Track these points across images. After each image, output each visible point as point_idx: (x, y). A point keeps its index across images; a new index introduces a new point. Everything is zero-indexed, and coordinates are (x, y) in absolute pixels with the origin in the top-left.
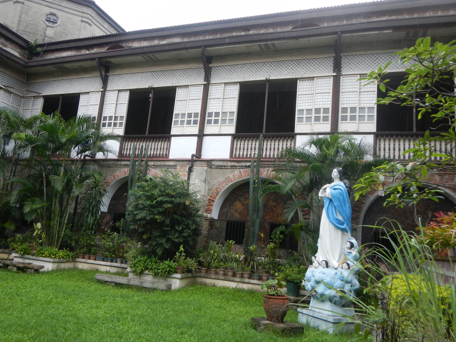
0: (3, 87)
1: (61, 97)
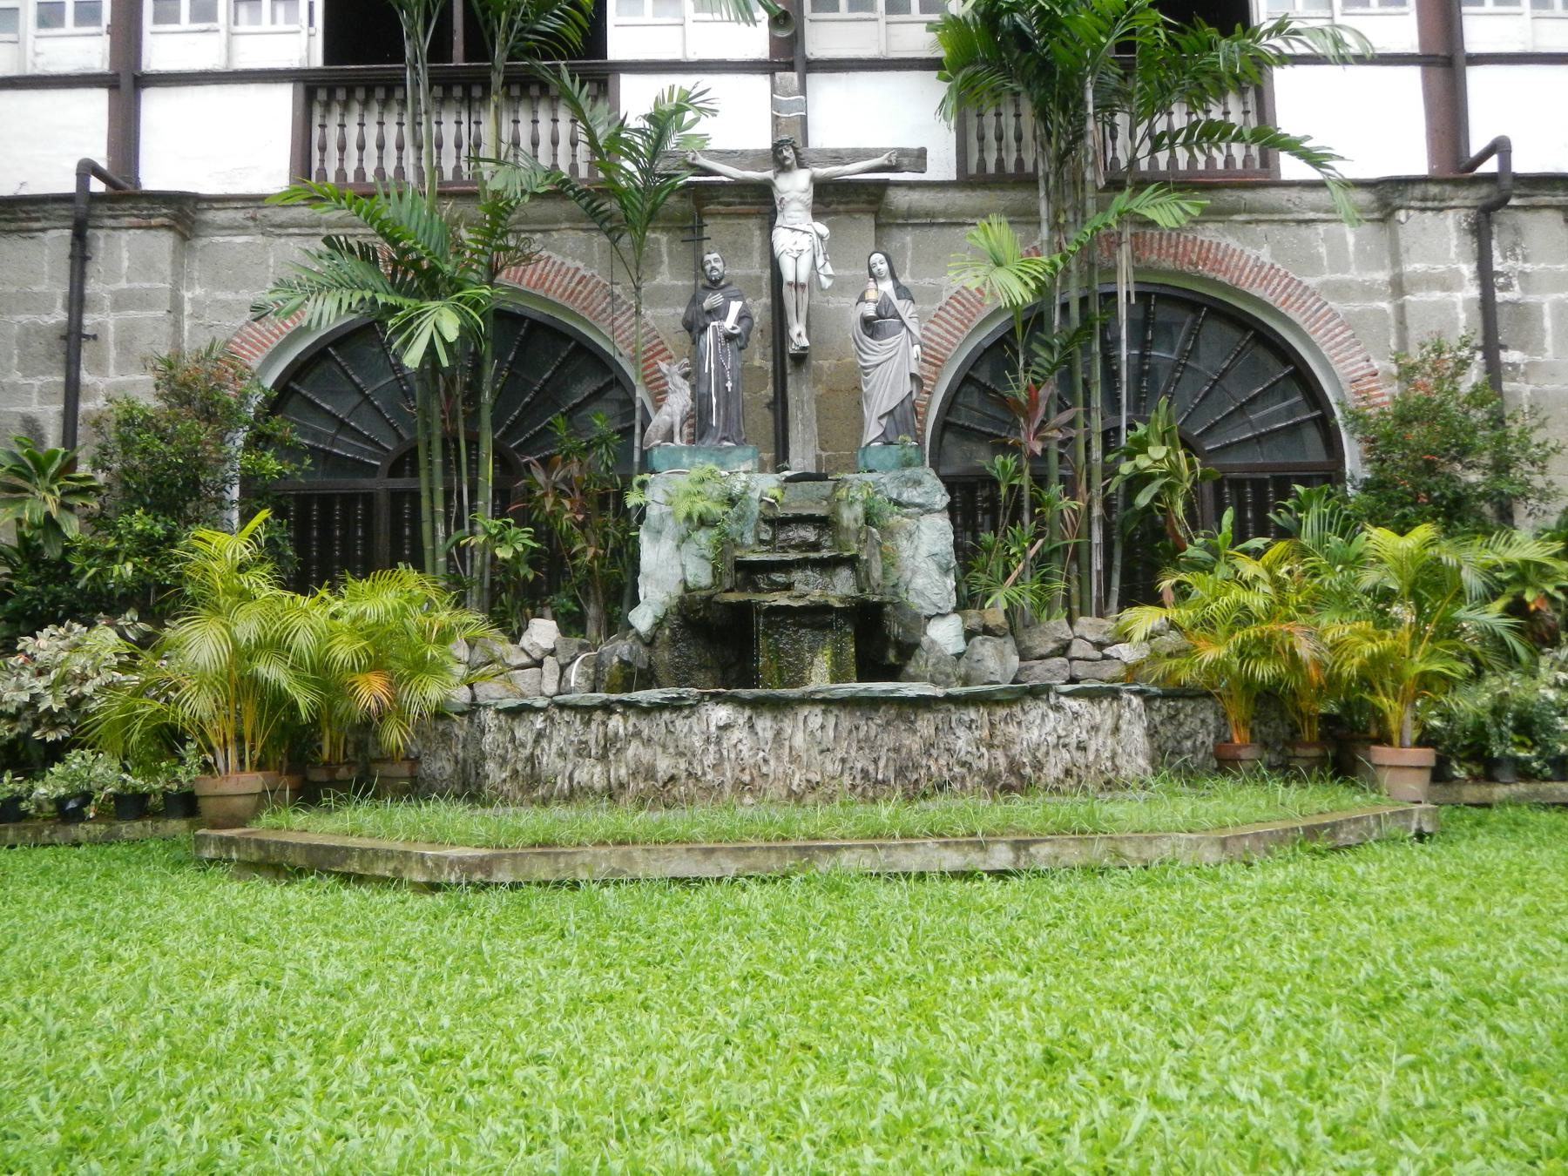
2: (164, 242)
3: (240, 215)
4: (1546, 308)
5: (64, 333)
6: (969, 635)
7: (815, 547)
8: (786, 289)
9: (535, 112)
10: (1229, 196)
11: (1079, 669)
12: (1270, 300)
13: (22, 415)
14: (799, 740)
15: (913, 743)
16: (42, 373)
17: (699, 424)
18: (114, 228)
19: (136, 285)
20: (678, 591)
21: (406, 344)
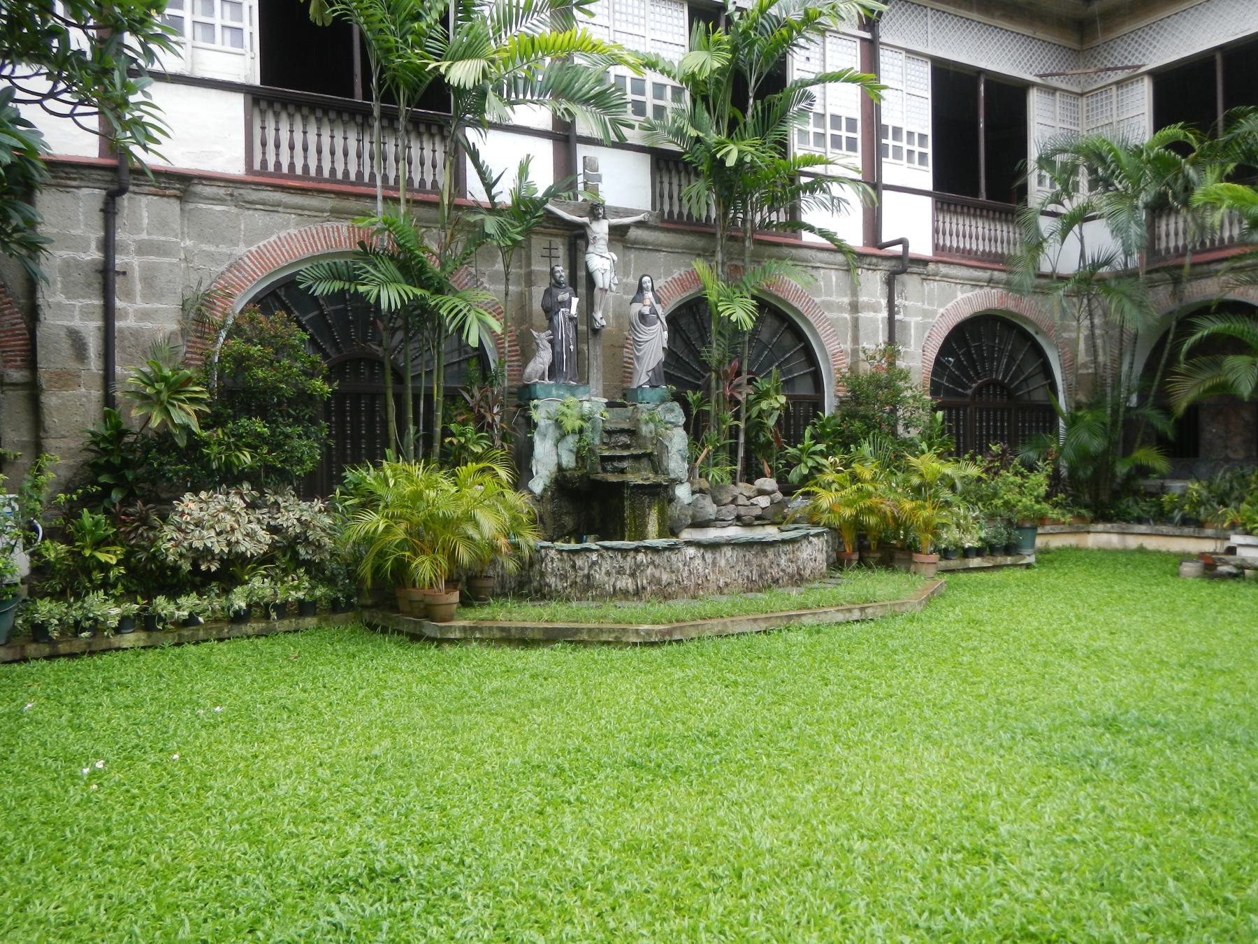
0: (1038, 80)
1: (1219, 57)
3: (222, 192)
5: (100, 267)
6: (693, 493)
7: (626, 447)
8: (596, 290)
9: (421, 143)
10: (786, 251)
11: (742, 511)
12: (800, 309)
13: (67, 328)
14: (723, 563)
15: (766, 562)
16: (83, 297)
17: (554, 370)
18: (135, 193)
19: (155, 237)
20: (554, 468)
21: (460, 329)
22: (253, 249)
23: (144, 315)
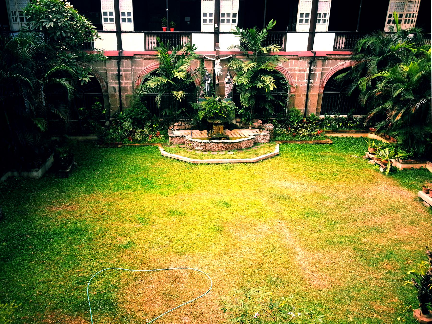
2: (129, 62)
4: (317, 74)
22: (146, 68)
23: (126, 83)
